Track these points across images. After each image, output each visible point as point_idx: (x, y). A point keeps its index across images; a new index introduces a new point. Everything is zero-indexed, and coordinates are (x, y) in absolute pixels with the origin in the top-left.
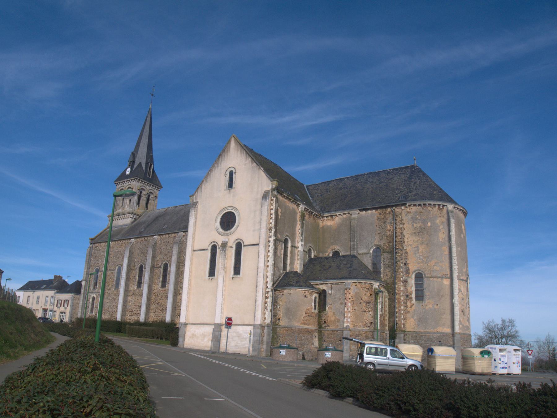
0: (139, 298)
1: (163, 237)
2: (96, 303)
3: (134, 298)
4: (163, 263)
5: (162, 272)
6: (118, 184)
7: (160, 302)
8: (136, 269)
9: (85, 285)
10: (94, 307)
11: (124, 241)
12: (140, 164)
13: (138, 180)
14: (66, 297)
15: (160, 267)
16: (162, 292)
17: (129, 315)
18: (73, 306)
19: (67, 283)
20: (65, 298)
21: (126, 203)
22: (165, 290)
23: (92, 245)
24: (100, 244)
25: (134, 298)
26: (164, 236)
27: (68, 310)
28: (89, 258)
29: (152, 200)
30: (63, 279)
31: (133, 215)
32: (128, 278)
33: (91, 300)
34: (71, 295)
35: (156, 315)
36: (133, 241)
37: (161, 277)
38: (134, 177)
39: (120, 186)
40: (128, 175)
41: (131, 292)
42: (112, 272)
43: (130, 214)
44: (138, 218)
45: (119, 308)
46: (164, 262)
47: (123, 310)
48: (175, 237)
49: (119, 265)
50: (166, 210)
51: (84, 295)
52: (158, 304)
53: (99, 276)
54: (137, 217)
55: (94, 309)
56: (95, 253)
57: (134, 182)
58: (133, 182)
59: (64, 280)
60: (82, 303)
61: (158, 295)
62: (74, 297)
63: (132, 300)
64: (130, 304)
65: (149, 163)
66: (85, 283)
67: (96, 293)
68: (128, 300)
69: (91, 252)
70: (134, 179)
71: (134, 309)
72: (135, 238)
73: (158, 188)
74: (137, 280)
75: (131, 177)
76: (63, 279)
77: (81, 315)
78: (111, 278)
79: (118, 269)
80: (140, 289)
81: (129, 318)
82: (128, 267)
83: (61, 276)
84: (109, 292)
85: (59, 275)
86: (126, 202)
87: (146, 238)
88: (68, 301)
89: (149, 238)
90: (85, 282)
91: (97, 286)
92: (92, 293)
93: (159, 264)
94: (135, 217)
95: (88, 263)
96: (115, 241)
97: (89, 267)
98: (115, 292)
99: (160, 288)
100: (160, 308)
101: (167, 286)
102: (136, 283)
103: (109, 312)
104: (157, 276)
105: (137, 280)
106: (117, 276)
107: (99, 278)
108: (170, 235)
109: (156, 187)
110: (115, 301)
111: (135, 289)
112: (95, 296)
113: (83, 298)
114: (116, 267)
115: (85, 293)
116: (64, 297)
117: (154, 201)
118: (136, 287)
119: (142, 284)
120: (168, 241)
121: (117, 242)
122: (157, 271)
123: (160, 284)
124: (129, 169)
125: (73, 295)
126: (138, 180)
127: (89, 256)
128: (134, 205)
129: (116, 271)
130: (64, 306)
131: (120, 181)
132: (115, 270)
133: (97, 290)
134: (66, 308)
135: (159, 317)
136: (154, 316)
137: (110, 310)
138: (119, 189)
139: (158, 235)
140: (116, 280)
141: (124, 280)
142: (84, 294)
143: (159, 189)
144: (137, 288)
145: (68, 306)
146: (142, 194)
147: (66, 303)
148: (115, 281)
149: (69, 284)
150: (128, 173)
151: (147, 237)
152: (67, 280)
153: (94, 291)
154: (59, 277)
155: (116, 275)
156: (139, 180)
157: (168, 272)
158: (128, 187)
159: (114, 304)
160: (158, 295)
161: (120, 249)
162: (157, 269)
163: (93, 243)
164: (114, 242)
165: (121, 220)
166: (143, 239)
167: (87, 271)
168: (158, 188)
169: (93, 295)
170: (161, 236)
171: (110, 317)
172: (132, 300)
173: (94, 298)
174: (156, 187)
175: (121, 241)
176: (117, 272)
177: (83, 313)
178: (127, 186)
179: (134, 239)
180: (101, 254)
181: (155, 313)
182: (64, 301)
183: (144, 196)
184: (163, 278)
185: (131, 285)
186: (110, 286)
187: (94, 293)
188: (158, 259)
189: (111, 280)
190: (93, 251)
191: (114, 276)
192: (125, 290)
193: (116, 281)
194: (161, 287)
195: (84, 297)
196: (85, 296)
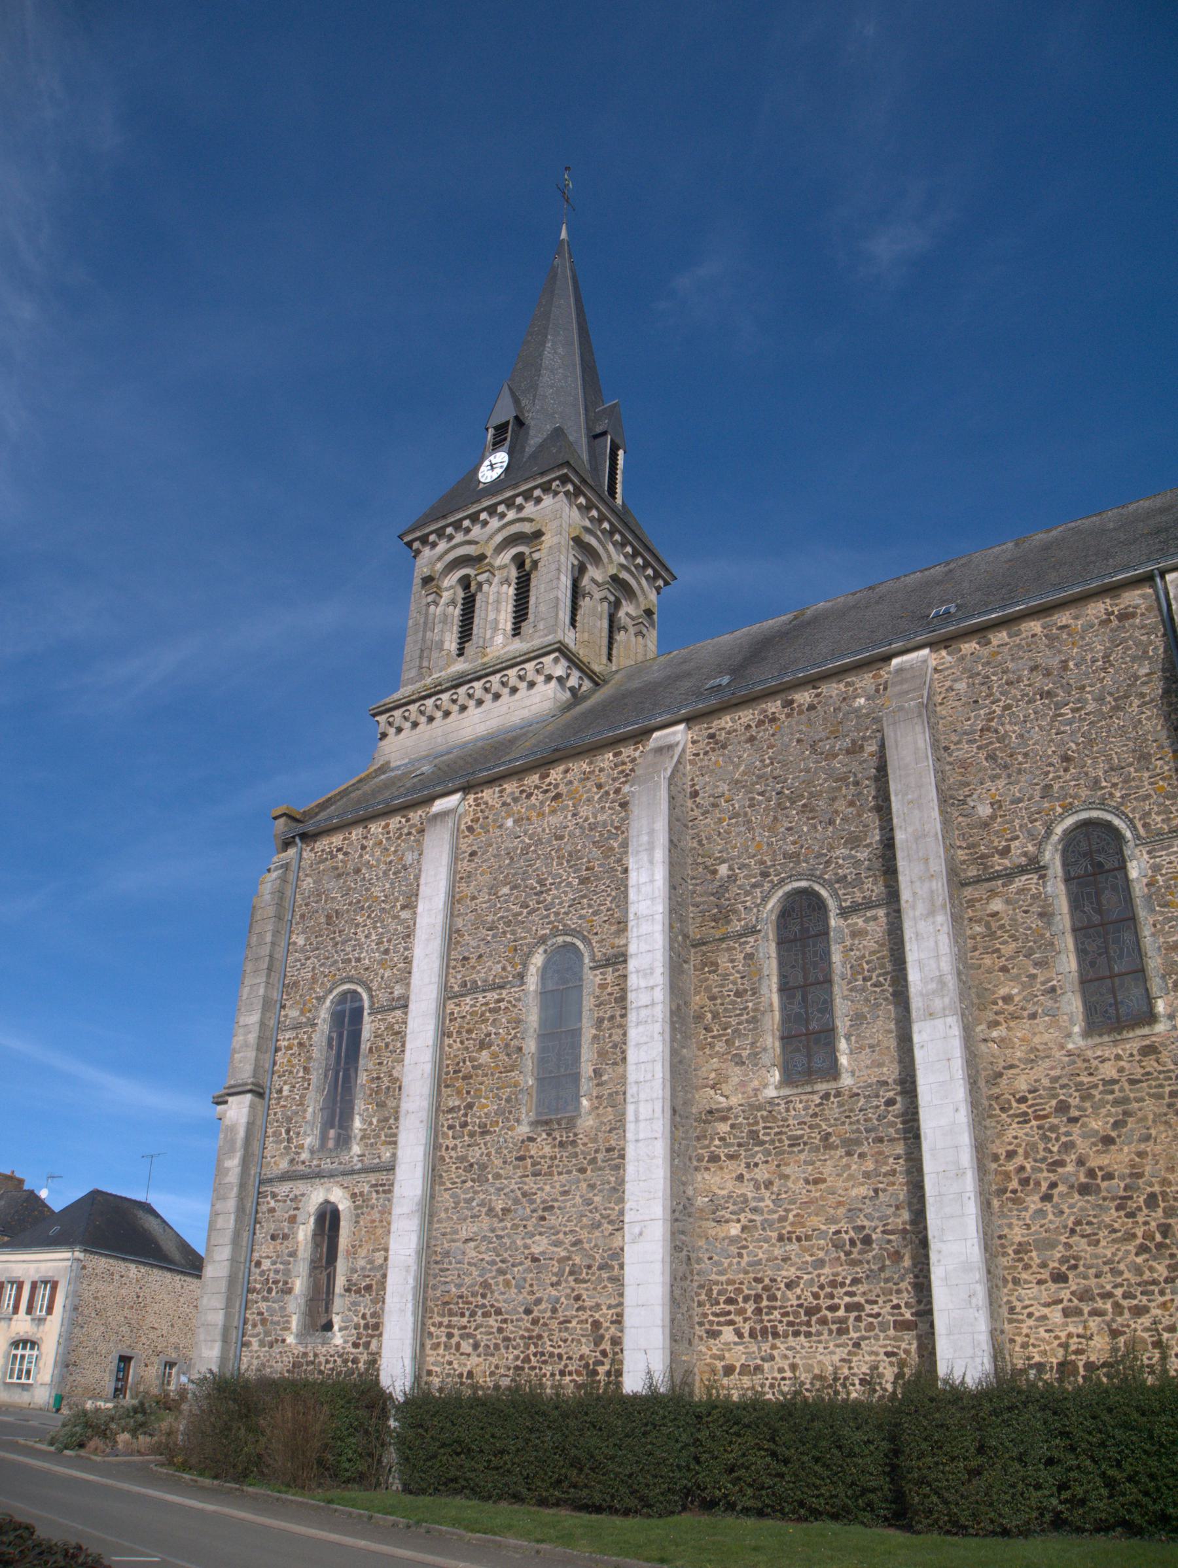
0: (828, 1170)
1: (985, 652)
2: (353, 1253)
3: (762, 1174)
4: (1059, 830)
5: (1062, 905)
6: (432, 538)
7: (1121, 1169)
8: (753, 931)
9: (250, 1125)
10: (340, 1282)
11: (580, 767)
12: (558, 433)
13: (570, 487)
14: (43, 1266)
15: (1035, 866)
16: (1109, 1071)
17: (728, 1334)
18: (76, 1309)
19: (47, 1206)
20: (37, 1270)
21: (496, 621)
22: (1149, 1050)
23: (292, 852)
24: (356, 833)
25: (762, 1174)
26: (1000, 637)
27: (51, 1333)
28: (276, 933)
29: (632, 630)
30: (26, 1187)
31: (564, 663)
32: (679, 1007)
33: (304, 1233)
34: (68, 1255)
35: (1084, 1295)
36: (679, 737)
37: (1068, 942)
38: (542, 474)
39: (442, 546)
40: (496, 487)
41: (723, 1128)
42: (493, 996)
43: (548, 660)
44: (592, 692)
45: (631, 1273)
46: (1070, 821)
47: (678, 1292)
48: (1124, 616)
49: (555, 932)
50: (796, 618)
51: (241, 1199)
52: (1084, 1190)
53: (364, 1046)
54: (587, 685)
55: (338, 1304)
56: (318, 894)
57: (548, 500)
58: (538, 500)
59: (32, 1192)
60: (233, 1260)
61: (1063, 1107)
62: (84, 1268)
63: (747, 1190)
64: (734, 1230)
65: (604, 434)
66: (252, 1106)
67: (352, 1172)
68: (701, 1201)
69: (289, 892)
70: (546, 488)
71: (791, 1272)
72: (689, 720)
73: (657, 575)
74: (777, 1015)
75: (526, 480)
76: (26, 1187)
77: (223, 1359)
78: (483, 1045)
79: (544, 972)
80: (822, 1087)
81: (738, 1356)
82: (671, 927)
83: (18, 1175)
84: (475, 1155)
85: (8, 1173)
86: (492, 616)
87: (803, 697)
88: (55, 1286)
89: (833, 689)
90: (249, 1096)
91: (357, 1124)
92: (316, 1175)
93: (1005, 852)
94: (573, 682)
95: (270, 969)
96: (491, 782)
97: (275, 995)
98: (543, 1148)
99: (1077, 1042)
100: (1122, 1223)
101: (1161, 1006)
102: (771, 1042)
103: (492, 1321)
104: (1009, 949)
105: (773, 1020)
106: (543, 1022)
107: (366, 1065)
108: (1064, 618)
109: (647, 565)
110: (552, 1220)
111: (771, 1092)
112: (339, 1197)
113: (239, 1219)
114: (529, 954)
115: (253, 1181)
116: (33, 1266)
117: (639, 633)
118: (776, 1076)
119: (843, 1045)
120: (1055, 662)
121: (510, 787)
122: (997, 905)
123: (1073, 1004)
124: (501, 458)
125: (79, 1255)
126: (570, 487)
127: (279, 917)
128: (561, 614)
129: (532, 982)
130: (29, 1311)
131: (444, 517)
132: (521, 976)
133: (356, 1149)
134: (41, 1321)
135: (1139, 1311)
136: (1066, 1313)
137: (510, 1299)
138: (439, 566)
139: (933, 645)
140: (542, 1049)
141: (658, 1027)
142: (242, 1186)
143: (660, 582)
144: (788, 1079)
145: (50, 1310)
146: (585, 581)
147: (43, 1293)
148: (529, 1064)
149: (53, 1212)
150: (487, 475)
151: (811, 682)
152: (44, 1194)
153: (326, 1165)
154: (10, 1178)
155: (533, 1018)
156: (578, 492)
157: (1139, 890)
158: (499, 538)
159: (540, 1245)
160: (1063, 1107)
161: (554, 820)
162: (993, 894)
163: (304, 837)
164: (489, 795)
165: (472, 709)
166: (774, 707)
167: (262, 1024)
168: (657, 575)
169: (316, 1196)
170: (969, 647)
171: (509, 1357)
172: (747, 1190)
173: (328, 1219)
174: (647, 565)
175: (556, 774)
176: (545, 994)
177: (234, 1334)
178: (491, 537)
179: (682, 727)
180: (376, 891)
181: (1074, 1283)
182: (34, 1286)
183: (598, 595)
184: (1081, 952)
185: (710, 1067)
186: (487, 1106)
187: (331, 1175)
188: (984, 811)
189: (484, 1056)
190: (308, 883)
191: (518, 1022)
192: (674, 1111)
193: (542, 1060)
194: (1087, 1033)
195: (240, 1209)
196: (249, 1205)
